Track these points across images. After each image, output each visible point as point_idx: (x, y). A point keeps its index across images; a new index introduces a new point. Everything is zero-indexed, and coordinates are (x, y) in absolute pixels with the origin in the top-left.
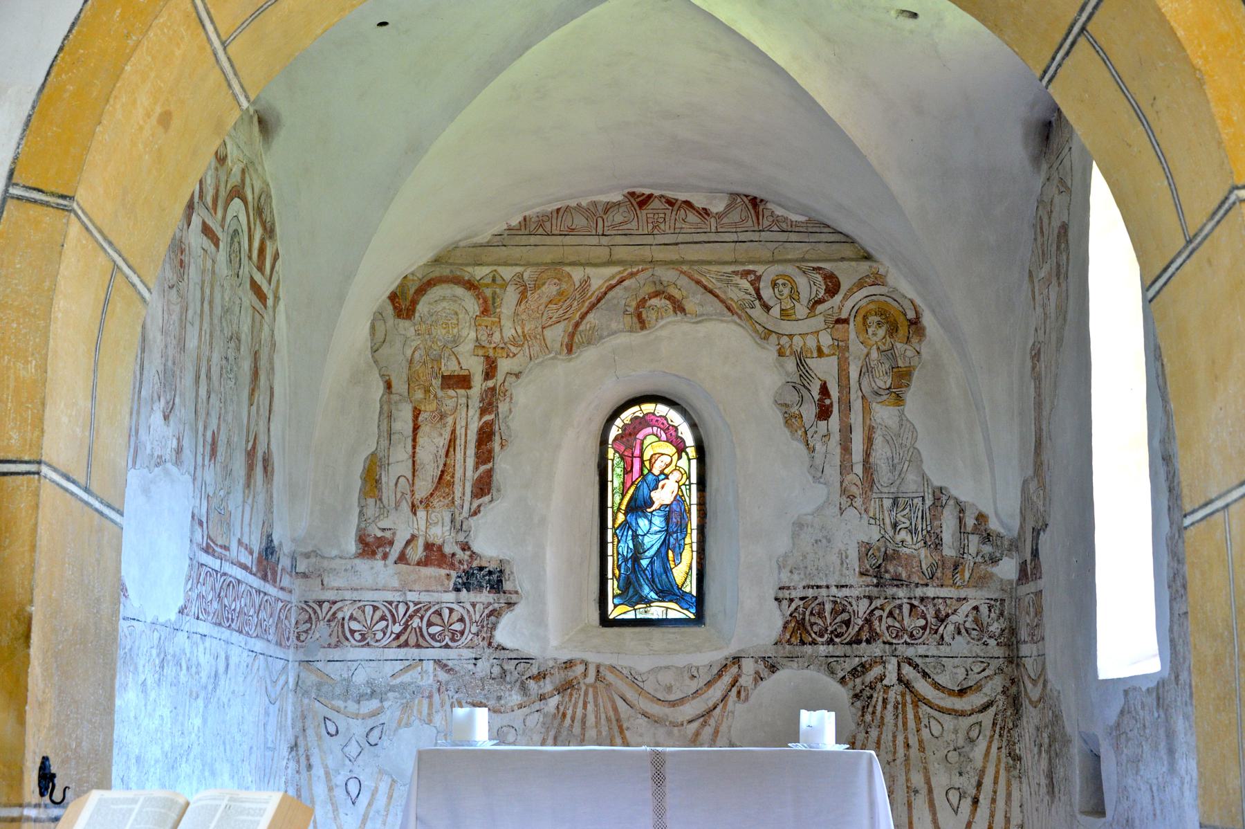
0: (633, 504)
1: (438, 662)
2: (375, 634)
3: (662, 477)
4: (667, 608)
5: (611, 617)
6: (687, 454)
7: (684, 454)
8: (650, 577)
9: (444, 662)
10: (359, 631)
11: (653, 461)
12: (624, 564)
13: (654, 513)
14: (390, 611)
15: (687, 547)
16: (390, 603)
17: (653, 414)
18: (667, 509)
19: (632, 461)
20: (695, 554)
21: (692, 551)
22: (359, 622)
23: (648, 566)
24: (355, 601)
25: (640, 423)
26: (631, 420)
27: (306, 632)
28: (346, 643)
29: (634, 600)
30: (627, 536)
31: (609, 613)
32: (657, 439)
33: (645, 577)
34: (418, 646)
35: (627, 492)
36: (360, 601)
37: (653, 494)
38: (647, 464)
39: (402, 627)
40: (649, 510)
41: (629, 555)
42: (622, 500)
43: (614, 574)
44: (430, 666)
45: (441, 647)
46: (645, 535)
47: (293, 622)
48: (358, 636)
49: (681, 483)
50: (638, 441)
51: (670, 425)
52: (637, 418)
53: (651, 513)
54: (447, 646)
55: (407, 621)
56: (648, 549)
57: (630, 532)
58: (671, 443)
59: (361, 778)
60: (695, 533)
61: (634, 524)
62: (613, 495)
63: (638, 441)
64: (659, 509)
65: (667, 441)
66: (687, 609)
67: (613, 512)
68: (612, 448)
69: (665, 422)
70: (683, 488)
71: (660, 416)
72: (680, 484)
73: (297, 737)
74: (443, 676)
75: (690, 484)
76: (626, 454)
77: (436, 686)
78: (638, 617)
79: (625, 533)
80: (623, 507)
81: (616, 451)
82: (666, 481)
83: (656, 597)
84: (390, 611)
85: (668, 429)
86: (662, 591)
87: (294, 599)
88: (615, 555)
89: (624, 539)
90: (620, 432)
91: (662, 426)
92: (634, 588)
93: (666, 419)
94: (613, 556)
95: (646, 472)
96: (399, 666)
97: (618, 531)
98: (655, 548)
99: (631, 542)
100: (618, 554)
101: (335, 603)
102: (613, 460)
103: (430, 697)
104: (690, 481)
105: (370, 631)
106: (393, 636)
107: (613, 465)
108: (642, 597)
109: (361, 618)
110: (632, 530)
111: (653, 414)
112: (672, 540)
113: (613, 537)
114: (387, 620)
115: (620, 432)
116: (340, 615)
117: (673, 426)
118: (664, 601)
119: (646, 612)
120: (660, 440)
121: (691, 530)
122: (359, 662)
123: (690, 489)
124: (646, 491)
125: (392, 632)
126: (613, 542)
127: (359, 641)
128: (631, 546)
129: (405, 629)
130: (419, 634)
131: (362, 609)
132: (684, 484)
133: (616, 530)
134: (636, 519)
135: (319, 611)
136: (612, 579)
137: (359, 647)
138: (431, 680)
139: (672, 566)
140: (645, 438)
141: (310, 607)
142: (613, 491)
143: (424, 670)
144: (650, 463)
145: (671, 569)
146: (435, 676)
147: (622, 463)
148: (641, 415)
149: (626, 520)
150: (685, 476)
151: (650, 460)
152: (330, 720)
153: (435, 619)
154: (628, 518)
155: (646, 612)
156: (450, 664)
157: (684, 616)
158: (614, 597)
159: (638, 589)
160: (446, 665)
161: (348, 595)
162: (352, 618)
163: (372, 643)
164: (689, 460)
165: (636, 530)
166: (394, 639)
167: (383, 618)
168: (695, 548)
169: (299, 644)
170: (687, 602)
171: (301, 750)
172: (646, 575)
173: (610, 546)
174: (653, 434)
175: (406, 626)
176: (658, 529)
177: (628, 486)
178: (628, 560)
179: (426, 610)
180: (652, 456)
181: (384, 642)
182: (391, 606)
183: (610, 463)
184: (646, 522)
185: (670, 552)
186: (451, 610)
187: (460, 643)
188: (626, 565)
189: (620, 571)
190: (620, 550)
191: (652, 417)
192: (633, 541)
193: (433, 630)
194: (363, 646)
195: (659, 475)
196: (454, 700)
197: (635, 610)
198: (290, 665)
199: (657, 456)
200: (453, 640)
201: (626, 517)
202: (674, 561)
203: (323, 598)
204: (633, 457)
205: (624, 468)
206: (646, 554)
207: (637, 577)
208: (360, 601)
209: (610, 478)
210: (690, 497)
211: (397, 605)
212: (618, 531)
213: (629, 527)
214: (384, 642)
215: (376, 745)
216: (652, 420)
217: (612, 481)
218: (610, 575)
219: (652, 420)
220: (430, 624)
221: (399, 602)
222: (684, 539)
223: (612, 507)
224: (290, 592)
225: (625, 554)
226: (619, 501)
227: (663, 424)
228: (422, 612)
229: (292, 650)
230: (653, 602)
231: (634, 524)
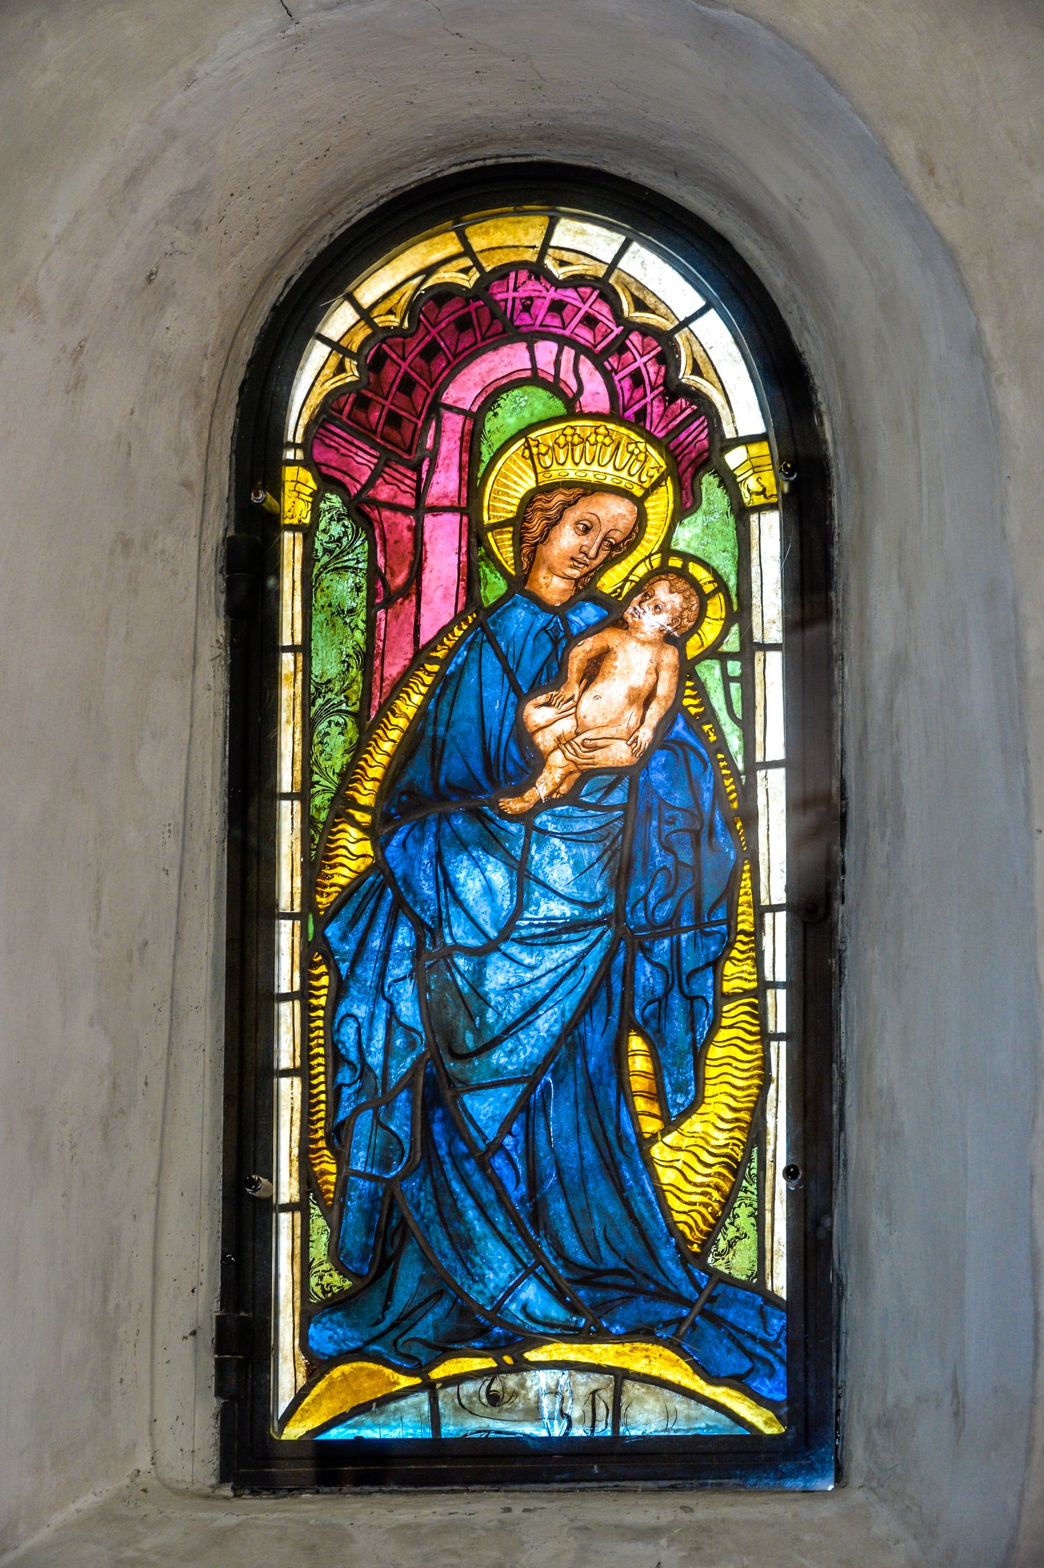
0: (418, 772)
3: (590, 613)
4: (621, 1376)
5: (294, 1431)
6: (729, 481)
7: (709, 483)
8: (516, 1192)
11: (536, 525)
12: (366, 1118)
13: (542, 819)
15: (734, 1013)
17: (537, 270)
18: (617, 797)
19: (418, 532)
20: (779, 1053)
21: (765, 1037)
23: (505, 1129)
25: (463, 324)
26: (413, 307)
29: (426, 1327)
30: (386, 955)
31: (283, 1406)
32: (558, 407)
33: (488, 1195)
35: (387, 707)
37: (536, 714)
38: (502, 544)
40: (514, 805)
41: (400, 1069)
42: (358, 750)
43: (308, 1180)
46: (491, 947)
49: (693, 648)
50: (453, 424)
51: (630, 326)
52: (445, 293)
53: (525, 818)
56: (509, 1030)
57: (404, 937)
58: (638, 422)
60: (777, 927)
61: (427, 889)
62: (309, 726)
63: (453, 424)
64: (572, 798)
65: (615, 415)
66: (738, 1382)
67: (308, 821)
68: (307, 463)
69: (603, 310)
70: (710, 673)
71: (576, 281)
72: (693, 648)
75: (750, 648)
76: (384, 492)
78: (449, 1429)
79: (376, 943)
80: (366, 794)
81: (327, 482)
82: (611, 638)
83: (557, 1312)
85: (620, 347)
86: (590, 1277)
88: (319, 1066)
89: (368, 972)
90: (352, 373)
91: (585, 335)
92: (426, 1259)
93: (609, 296)
94: (303, 1071)
95: (494, 588)
97: (332, 931)
98: (547, 1022)
99: (408, 989)
100: (337, 1058)
102: (308, 532)
104: (746, 635)
107: (309, 559)
108: (464, 1309)
110: (418, 925)
111: (537, 270)
112: (646, 974)
113: (307, 966)
115: (352, 373)
117: (646, 330)
118: (601, 1336)
119: (494, 1399)
120: (573, 409)
121: (760, 911)
123: (747, 681)
124: (495, 696)
126: (304, 995)
128: (408, 1010)
132: (714, 652)
133: (322, 923)
134: (438, 858)
136: (300, 1207)
139: (650, 1126)
140: (491, 398)
142: (308, 700)
144: (518, 540)
145: (645, 1143)
147: (361, 548)
148: (468, 281)
149: (379, 866)
150: (716, 608)
151: (518, 524)
154: (393, 850)
155: (494, 1399)
157: (721, 1425)
158: (307, 1316)
159: (449, 1261)
164: (741, 513)
165: (441, 920)
168: (779, 1020)
170: (736, 1337)
172: (494, 1181)
173: (287, 1015)
174: (535, 379)
176: (558, 909)
177: (393, 671)
178: (389, 1100)
180: (528, 501)
183: (291, 547)
184: (499, 876)
185: (636, 1043)
188: (378, 1123)
189: (341, 1158)
190: (349, 1033)
191: (531, 287)
192: (422, 989)
195: (571, 604)
197: (429, 1387)
199: (559, 498)
201: (380, 844)
202: (658, 1095)
204: (420, 508)
205: (374, 574)
206: (498, 1057)
207: (441, 1193)
209: (290, 631)
210: (746, 725)
212: (332, 931)
213: (399, 906)
216: (527, 305)
217: (304, 649)
218: (288, 1189)
219: (527, 305)
222: (715, 964)
223: (303, 795)
225: (375, 1060)
226: (339, 761)
227: (590, 321)
230: (536, 1342)
231: (427, 889)
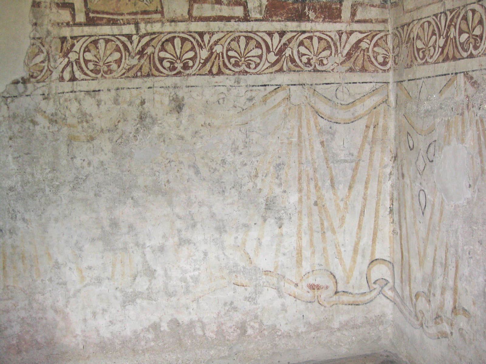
1: (466, 74)
2: (429, 50)
9: (470, 73)
10: (422, 49)
14: (436, 23)
16: (436, 15)
22: (421, 40)
24: (419, 20)
27: (397, 55)
28: (416, 63)
34: (454, 59)
36: (421, 19)
39: (444, 40)
44: (461, 78)
45: (467, 57)
47: (391, 47)
48: (421, 55)
54: (471, 56)
55: (447, 33)
59: (426, 191)
73: (397, 149)
74: (471, 90)
77: (466, 101)
84: (436, 23)
87: (390, 27)
96: (443, 81)
101: (409, 24)
103: (462, 114)
105: (427, 48)
106: (440, 49)
109: (422, 37)
114: (435, 35)
116: (412, 36)
122: (423, 79)
125: (439, 47)
127: (422, 59)
129: (446, 42)
130: (454, 45)
131: (422, 26)
135: (402, 35)
137: (421, 65)
138: (462, 97)
141: (399, 31)
143: (458, 83)
146: (465, 90)
152: (410, 135)
153: (464, 27)
156: (474, 75)
160: (472, 78)
161: (416, 15)
162: (418, 37)
163: (429, 60)
166: (441, 54)
167: (434, 34)
169: (396, 66)
171: (399, 159)
175: (447, 37)
179: (458, 18)
181: (435, 57)
182: (437, 18)
186: (474, 11)
187: (480, 49)
193: (465, 36)
194: (424, 64)
196: (478, 118)
198: (391, 86)
200: (476, 48)
203: (405, 22)
208: (421, 19)
211: (440, 16)
214: (435, 57)
215: (432, 161)
220: (461, 32)
221: (441, 13)
224: (384, 21)
228: (455, 20)
229: (391, 73)
